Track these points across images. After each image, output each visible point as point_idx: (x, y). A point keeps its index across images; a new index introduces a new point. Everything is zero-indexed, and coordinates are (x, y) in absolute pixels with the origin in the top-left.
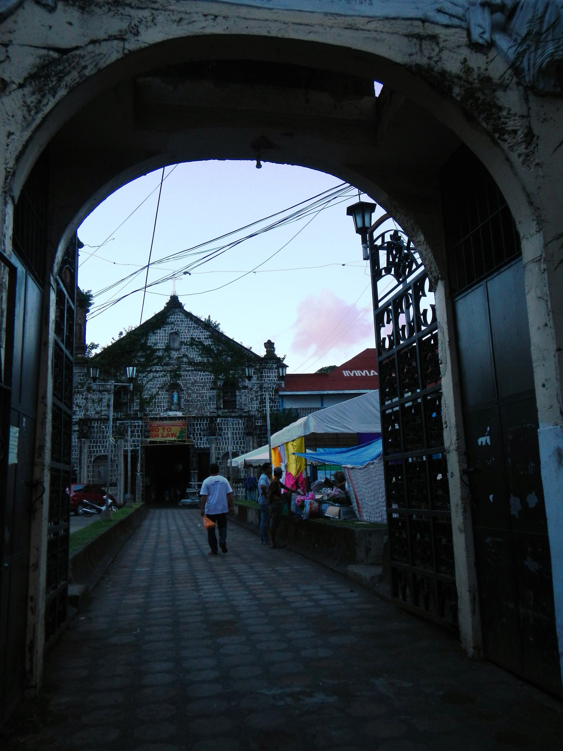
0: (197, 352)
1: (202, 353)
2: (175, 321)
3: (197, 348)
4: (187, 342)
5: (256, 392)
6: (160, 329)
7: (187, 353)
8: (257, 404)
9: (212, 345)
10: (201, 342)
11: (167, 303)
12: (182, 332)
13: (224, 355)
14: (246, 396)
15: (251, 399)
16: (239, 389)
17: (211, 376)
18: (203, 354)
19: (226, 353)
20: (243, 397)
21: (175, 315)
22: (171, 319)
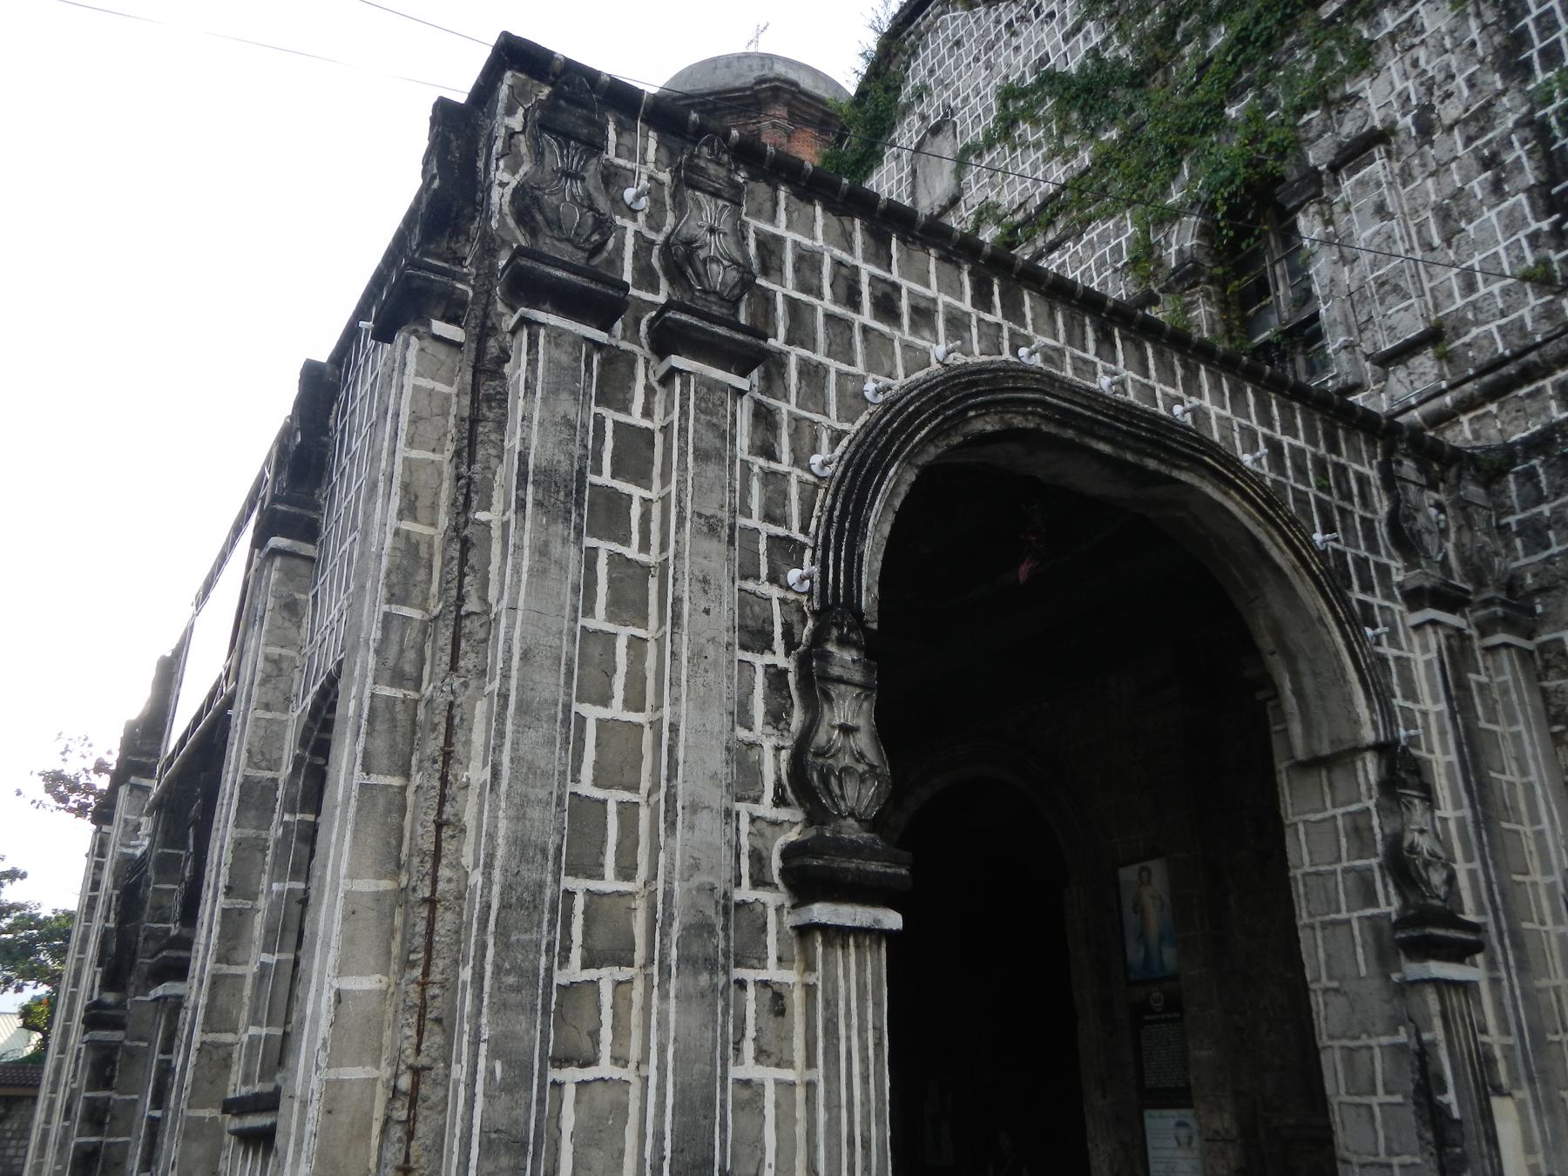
0: (1037, 145)
1: (1064, 132)
2: (932, 72)
3: (1036, 122)
4: (987, 134)
5: (1483, 116)
6: (878, 158)
7: (992, 196)
8: (1512, 223)
9: (1106, 42)
10: (1049, 79)
11: (895, 17)
12: (966, 100)
13: (1188, 38)
14: (1381, 211)
15: (1444, 214)
16: (1314, 185)
17: (1119, 229)
18: (1064, 132)
19: (1195, 18)
20: (1365, 232)
21: (925, 48)
22: (917, 74)
